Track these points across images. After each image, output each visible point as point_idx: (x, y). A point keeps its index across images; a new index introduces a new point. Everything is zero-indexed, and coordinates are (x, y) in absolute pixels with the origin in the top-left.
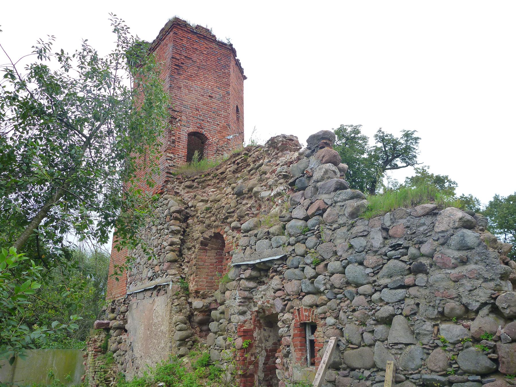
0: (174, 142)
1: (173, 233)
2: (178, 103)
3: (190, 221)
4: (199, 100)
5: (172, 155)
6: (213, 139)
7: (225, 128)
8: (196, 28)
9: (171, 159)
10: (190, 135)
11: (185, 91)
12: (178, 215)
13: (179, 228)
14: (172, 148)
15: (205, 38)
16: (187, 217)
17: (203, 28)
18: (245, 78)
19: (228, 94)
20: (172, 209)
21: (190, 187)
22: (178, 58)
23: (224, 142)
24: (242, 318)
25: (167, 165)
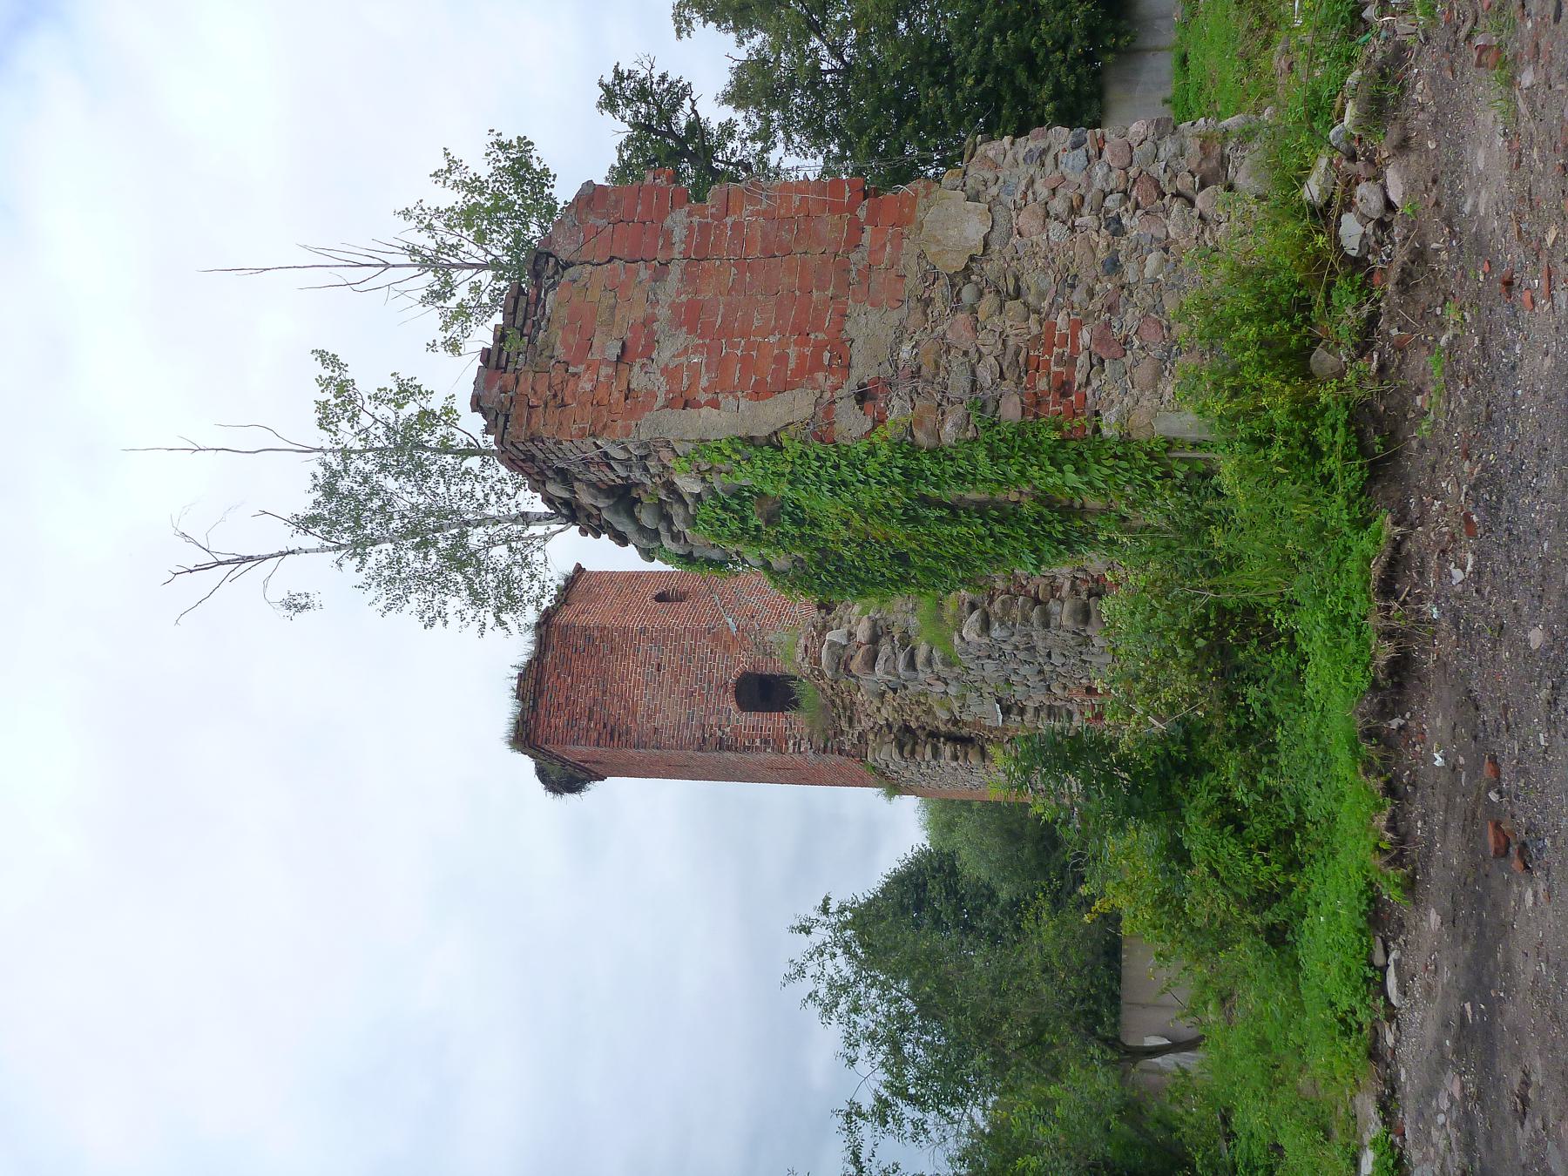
0: (766, 742)
1: (936, 754)
2: (686, 733)
3: (913, 725)
4: (671, 692)
5: (791, 743)
6: (743, 662)
7: (716, 637)
8: (523, 700)
9: (797, 744)
10: (745, 705)
11: (659, 721)
12: (907, 749)
13: (929, 748)
14: (777, 743)
15: (538, 682)
16: (907, 729)
17: (519, 686)
18: (579, 569)
19: (643, 631)
20: (896, 757)
21: (851, 720)
22: (596, 735)
23: (744, 639)
24: (1077, 717)
25: (810, 752)
